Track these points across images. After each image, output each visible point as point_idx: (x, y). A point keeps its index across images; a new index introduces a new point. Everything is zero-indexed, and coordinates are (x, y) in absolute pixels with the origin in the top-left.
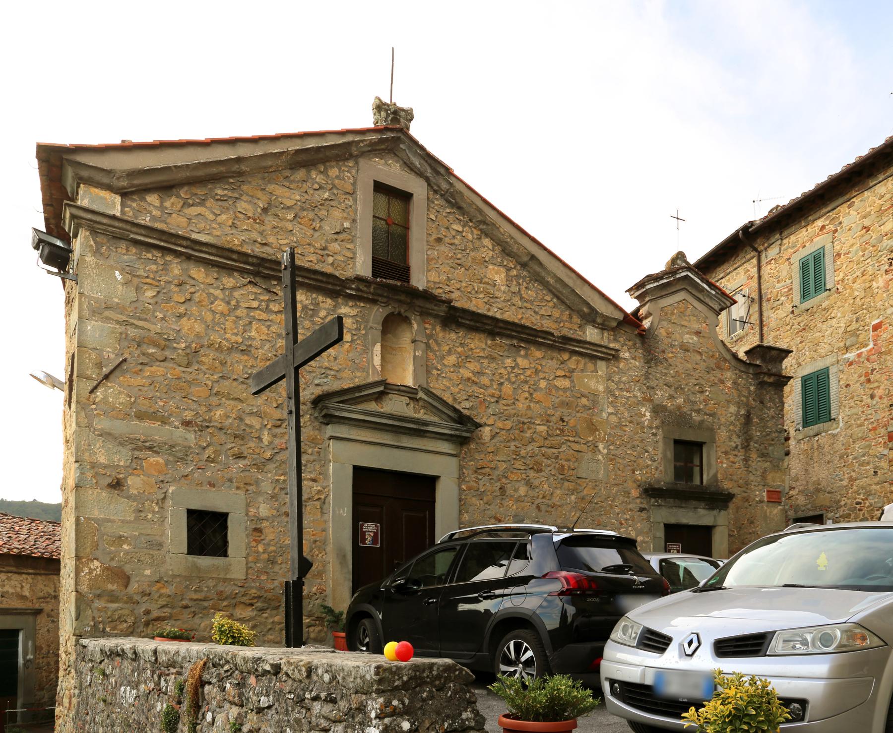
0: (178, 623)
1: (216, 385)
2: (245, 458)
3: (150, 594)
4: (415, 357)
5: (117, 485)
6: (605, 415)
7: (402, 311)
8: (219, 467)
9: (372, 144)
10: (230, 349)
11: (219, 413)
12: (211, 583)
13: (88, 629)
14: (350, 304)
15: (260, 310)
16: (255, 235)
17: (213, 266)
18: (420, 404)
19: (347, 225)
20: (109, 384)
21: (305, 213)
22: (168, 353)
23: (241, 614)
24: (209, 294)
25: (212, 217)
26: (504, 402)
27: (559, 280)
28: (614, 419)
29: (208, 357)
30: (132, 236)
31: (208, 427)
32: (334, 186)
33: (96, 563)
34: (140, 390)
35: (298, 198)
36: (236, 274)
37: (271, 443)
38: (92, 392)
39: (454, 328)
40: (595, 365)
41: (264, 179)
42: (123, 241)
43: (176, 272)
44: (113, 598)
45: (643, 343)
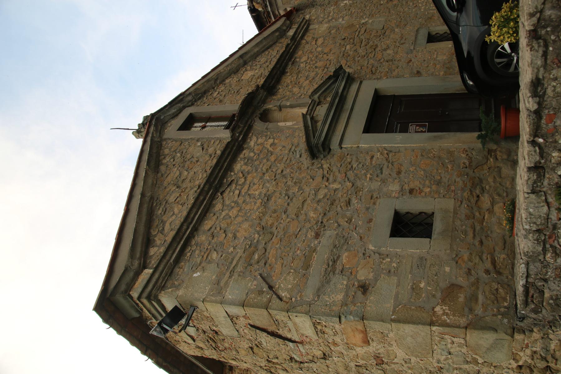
0: (497, 248)
1: (290, 216)
2: (349, 199)
3: (469, 269)
4: (292, 106)
5: (364, 288)
6: (344, 22)
7: (259, 112)
8: (356, 216)
9: (156, 130)
10: (265, 208)
11: (312, 214)
12: (458, 223)
13: (506, 321)
14: (249, 140)
15: (242, 189)
16: (193, 191)
17: (205, 215)
18: (322, 100)
19: (199, 144)
20: (277, 286)
21: (186, 166)
22: (261, 247)
23: (487, 204)
24: (224, 218)
25: (174, 217)
26: (328, 65)
27: (257, 45)
28: (346, 18)
29: (268, 220)
30: (172, 261)
31: (322, 222)
32: (175, 151)
33: (438, 309)
34: (285, 266)
35: (176, 169)
36: (214, 202)
37: (340, 183)
38: (281, 299)
39: (276, 90)
40: (312, 29)
41: (159, 187)
42: (175, 270)
43: (203, 238)
44: (473, 298)
45: (302, 10)
